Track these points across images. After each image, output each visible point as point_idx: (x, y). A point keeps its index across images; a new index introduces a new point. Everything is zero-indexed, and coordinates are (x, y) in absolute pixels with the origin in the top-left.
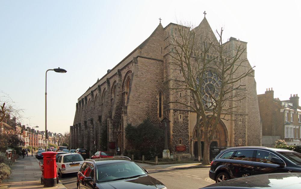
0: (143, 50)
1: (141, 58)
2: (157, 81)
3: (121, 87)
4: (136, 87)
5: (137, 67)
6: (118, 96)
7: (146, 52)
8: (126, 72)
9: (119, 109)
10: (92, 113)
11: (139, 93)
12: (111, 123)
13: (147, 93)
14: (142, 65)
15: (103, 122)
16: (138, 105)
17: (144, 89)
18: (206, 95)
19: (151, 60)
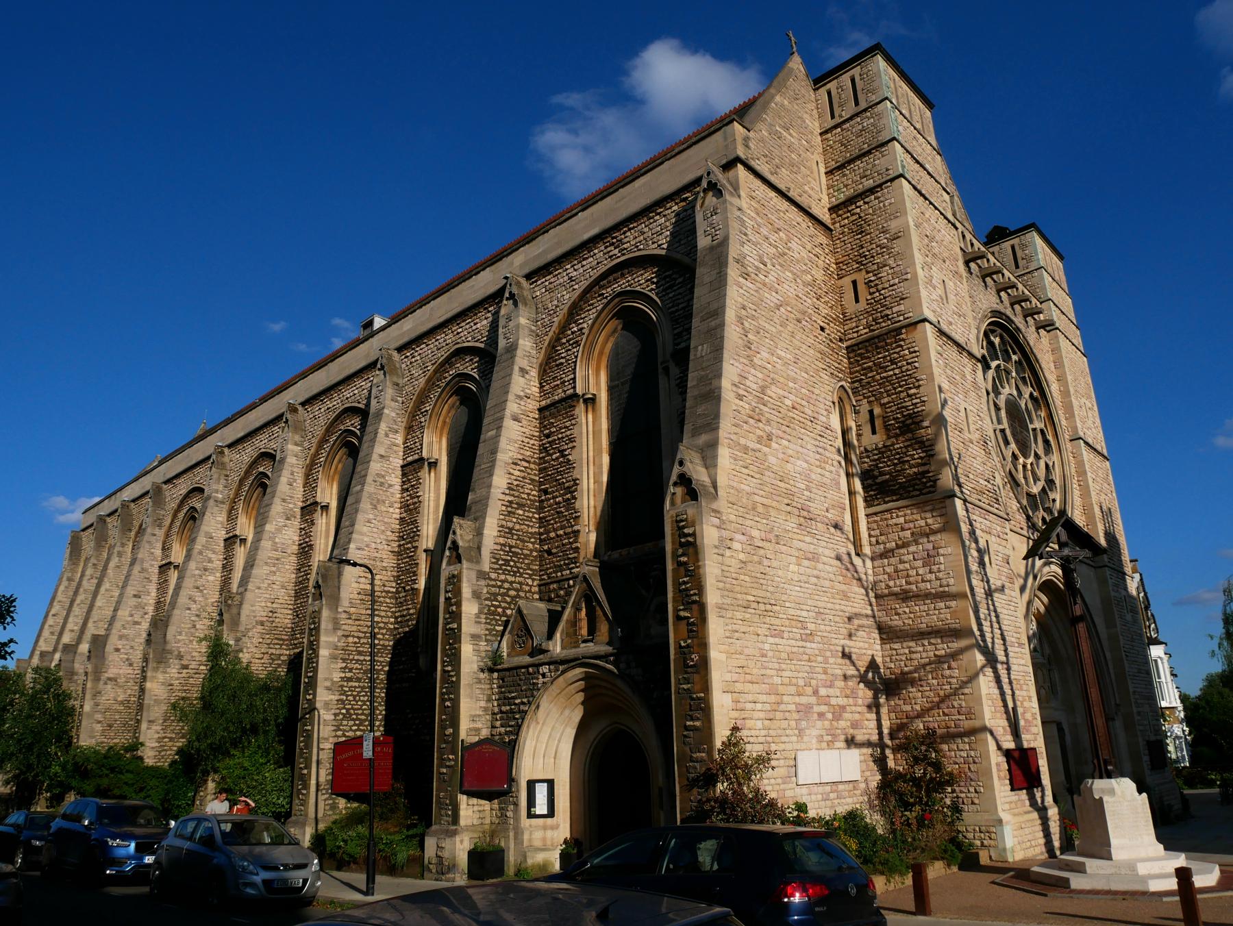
0: (751, 134)
2: (822, 329)
3: (534, 373)
5: (738, 213)
6: (516, 419)
8: (595, 274)
9: (521, 506)
10: (206, 570)
12: (476, 595)
15: (352, 605)
17: (779, 352)
19: (785, 205)
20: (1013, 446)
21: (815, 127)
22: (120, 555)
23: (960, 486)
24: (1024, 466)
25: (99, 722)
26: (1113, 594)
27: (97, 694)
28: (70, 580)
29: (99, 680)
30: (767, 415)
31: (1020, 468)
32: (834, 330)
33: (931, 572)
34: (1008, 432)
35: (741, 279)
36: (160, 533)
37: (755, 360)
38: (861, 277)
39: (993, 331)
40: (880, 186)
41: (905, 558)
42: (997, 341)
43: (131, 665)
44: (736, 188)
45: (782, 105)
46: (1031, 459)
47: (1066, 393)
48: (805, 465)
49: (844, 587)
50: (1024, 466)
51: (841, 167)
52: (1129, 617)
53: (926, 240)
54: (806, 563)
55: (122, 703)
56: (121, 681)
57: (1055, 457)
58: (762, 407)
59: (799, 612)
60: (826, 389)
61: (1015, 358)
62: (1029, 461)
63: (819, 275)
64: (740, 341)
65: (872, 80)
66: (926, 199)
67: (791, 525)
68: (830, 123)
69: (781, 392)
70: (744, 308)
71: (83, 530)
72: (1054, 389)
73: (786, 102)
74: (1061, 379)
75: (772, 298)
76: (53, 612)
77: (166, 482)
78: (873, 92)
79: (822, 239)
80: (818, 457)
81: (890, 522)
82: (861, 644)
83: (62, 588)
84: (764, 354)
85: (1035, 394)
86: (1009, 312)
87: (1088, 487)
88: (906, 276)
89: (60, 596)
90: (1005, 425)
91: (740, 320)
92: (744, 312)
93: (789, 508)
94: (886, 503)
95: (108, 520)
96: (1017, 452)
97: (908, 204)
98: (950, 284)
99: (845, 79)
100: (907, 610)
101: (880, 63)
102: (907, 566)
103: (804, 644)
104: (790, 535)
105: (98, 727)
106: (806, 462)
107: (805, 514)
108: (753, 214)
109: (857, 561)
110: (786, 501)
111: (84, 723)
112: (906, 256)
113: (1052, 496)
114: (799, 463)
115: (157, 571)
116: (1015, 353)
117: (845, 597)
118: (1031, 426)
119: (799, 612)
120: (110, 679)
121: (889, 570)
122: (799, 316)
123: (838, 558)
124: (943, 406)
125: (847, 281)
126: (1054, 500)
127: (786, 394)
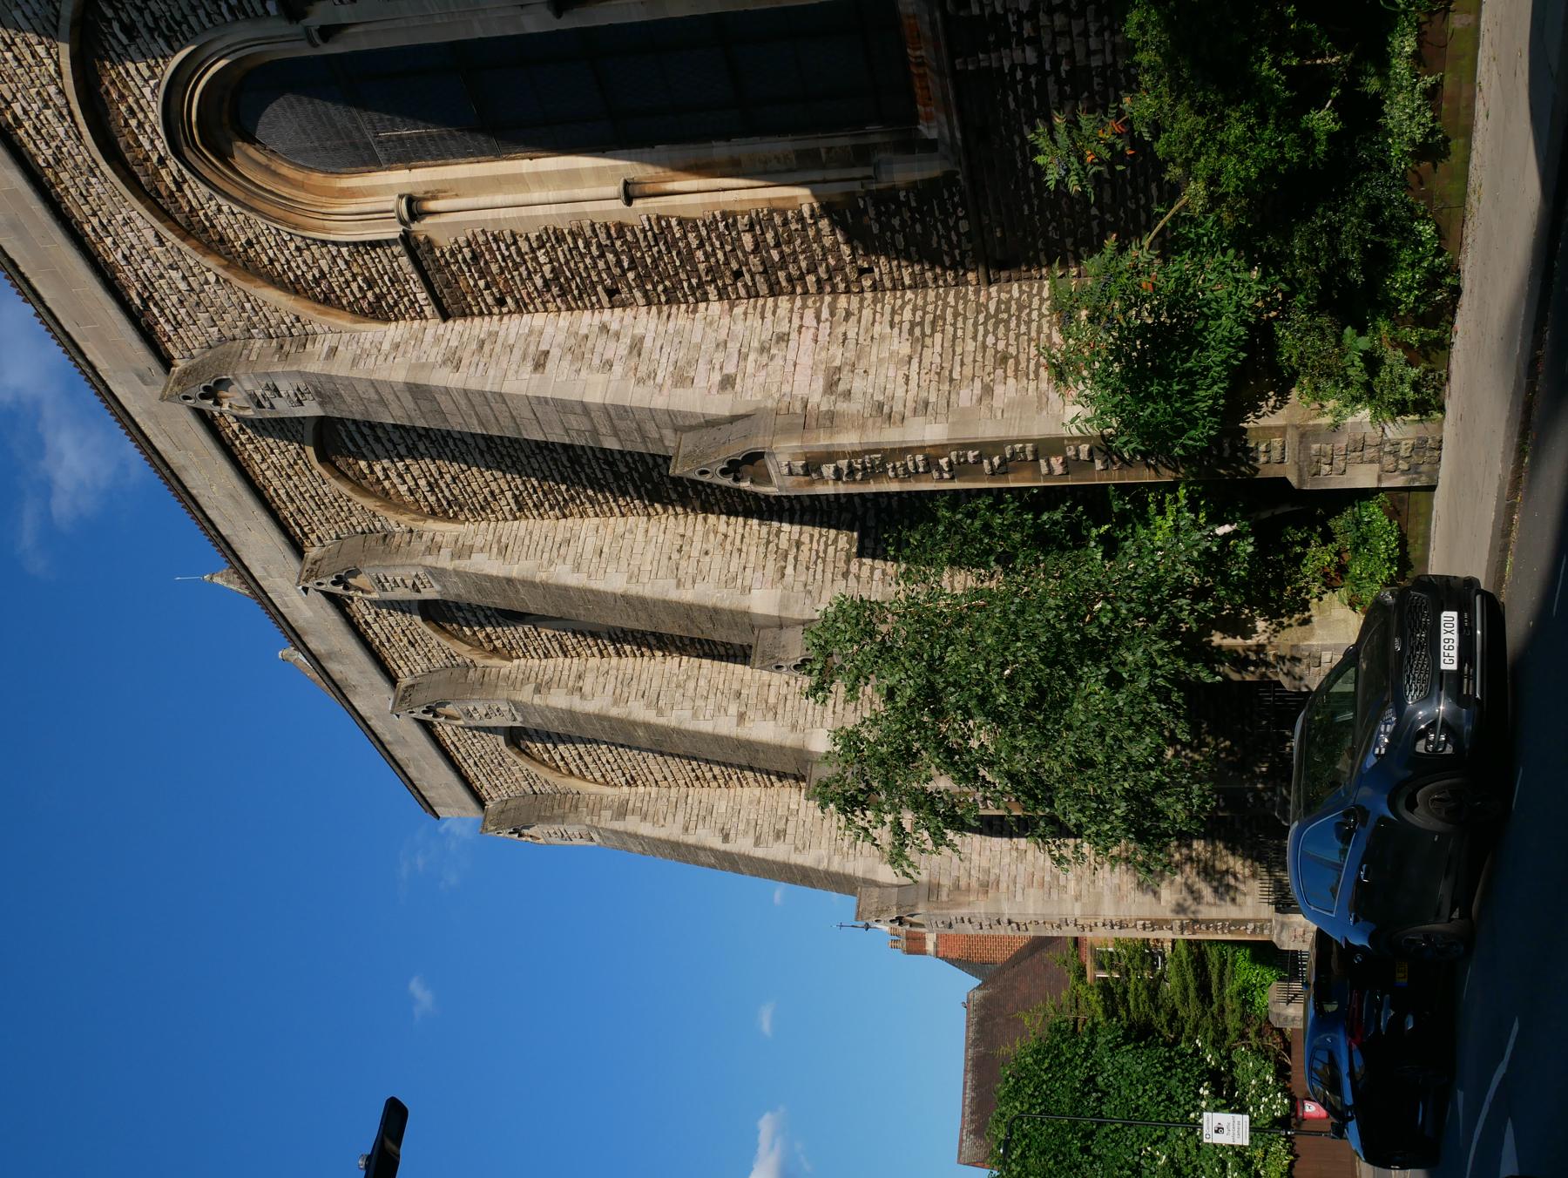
22: (463, 551)
25: (988, 390)
27: (883, 412)
28: (622, 811)
29: (831, 416)
36: (323, 322)
43: (783, 338)
55: (919, 342)
56: (837, 355)
71: (480, 801)
76: (716, 843)
77: (166, 362)
83: (646, 829)
89: (671, 830)
95: (405, 681)
105: (1006, 391)
111: (988, 431)
115: (459, 325)
120: (831, 386)
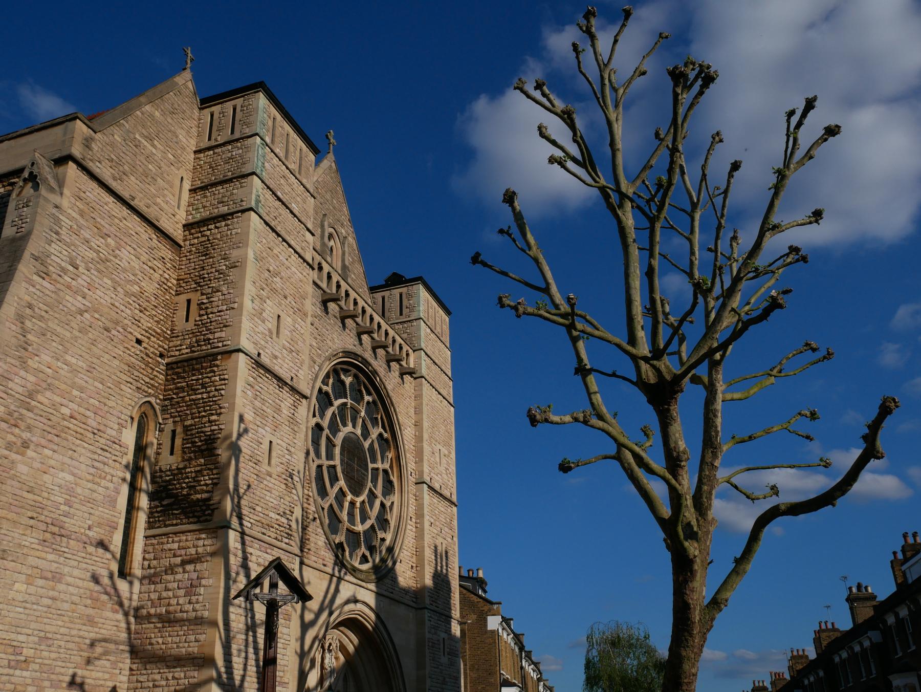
0: (98, 136)
1: (85, 178)
2: (139, 342)
4: (24, 332)
5: (54, 211)
7: (111, 160)
11: (32, 378)
13: (75, 393)
14: (82, 214)
16: (14, 456)
17: (68, 358)
18: (341, 489)
19: (126, 212)
20: (342, 483)
21: (192, 145)
23: (240, 517)
24: (352, 503)
26: (428, 635)
30: (29, 421)
31: (346, 505)
32: (154, 345)
33: (190, 603)
34: (339, 469)
35: (35, 277)
37: (30, 362)
38: (195, 297)
39: (346, 371)
40: (232, 214)
41: (170, 586)
42: (348, 380)
44: (61, 183)
45: (151, 116)
46: (363, 497)
47: (419, 439)
48: (70, 478)
49: (90, 611)
50: (352, 503)
51: (204, 188)
52: (444, 660)
53: (267, 274)
54: (41, 582)
57: (395, 498)
58: (24, 412)
59: (13, 636)
60: (127, 402)
61: (367, 398)
62: (359, 500)
63: (151, 288)
64: (14, 340)
65: (250, 113)
66: (279, 235)
67: (30, 540)
68: (205, 143)
69: (58, 399)
70: (30, 306)
72: (407, 435)
73: (157, 114)
74: (418, 425)
75: (73, 302)
78: (248, 125)
79: (166, 252)
80: (92, 471)
81: (166, 547)
82: (100, 675)
84: (46, 358)
85: (385, 435)
86: (368, 355)
87: (423, 530)
88: (233, 306)
90: (337, 462)
91: (20, 318)
92: (28, 311)
93: (32, 522)
94: (166, 526)
96: (346, 489)
97: (252, 237)
98: (287, 321)
99: (229, 105)
100: (160, 640)
101: (262, 100)
102: (170, 594)
103: (11, 671)
104: (25, 551)
106: (74, 475)
107: (55, 529)
108: (74, 214)
109: (123, 585)
110: (30, 514)
112: (237, 286)
113: (380, 534)
114: (61, 475)
116: (369, 394)
117: (91, 621)
118: (371, 466)
119: (13, 636)
121: (154, 596)
122: (109, 324)
123: (96, 579)
124: (240, 436)
125: (183, 298)
126: (383, 540)
127: (65, 402)
